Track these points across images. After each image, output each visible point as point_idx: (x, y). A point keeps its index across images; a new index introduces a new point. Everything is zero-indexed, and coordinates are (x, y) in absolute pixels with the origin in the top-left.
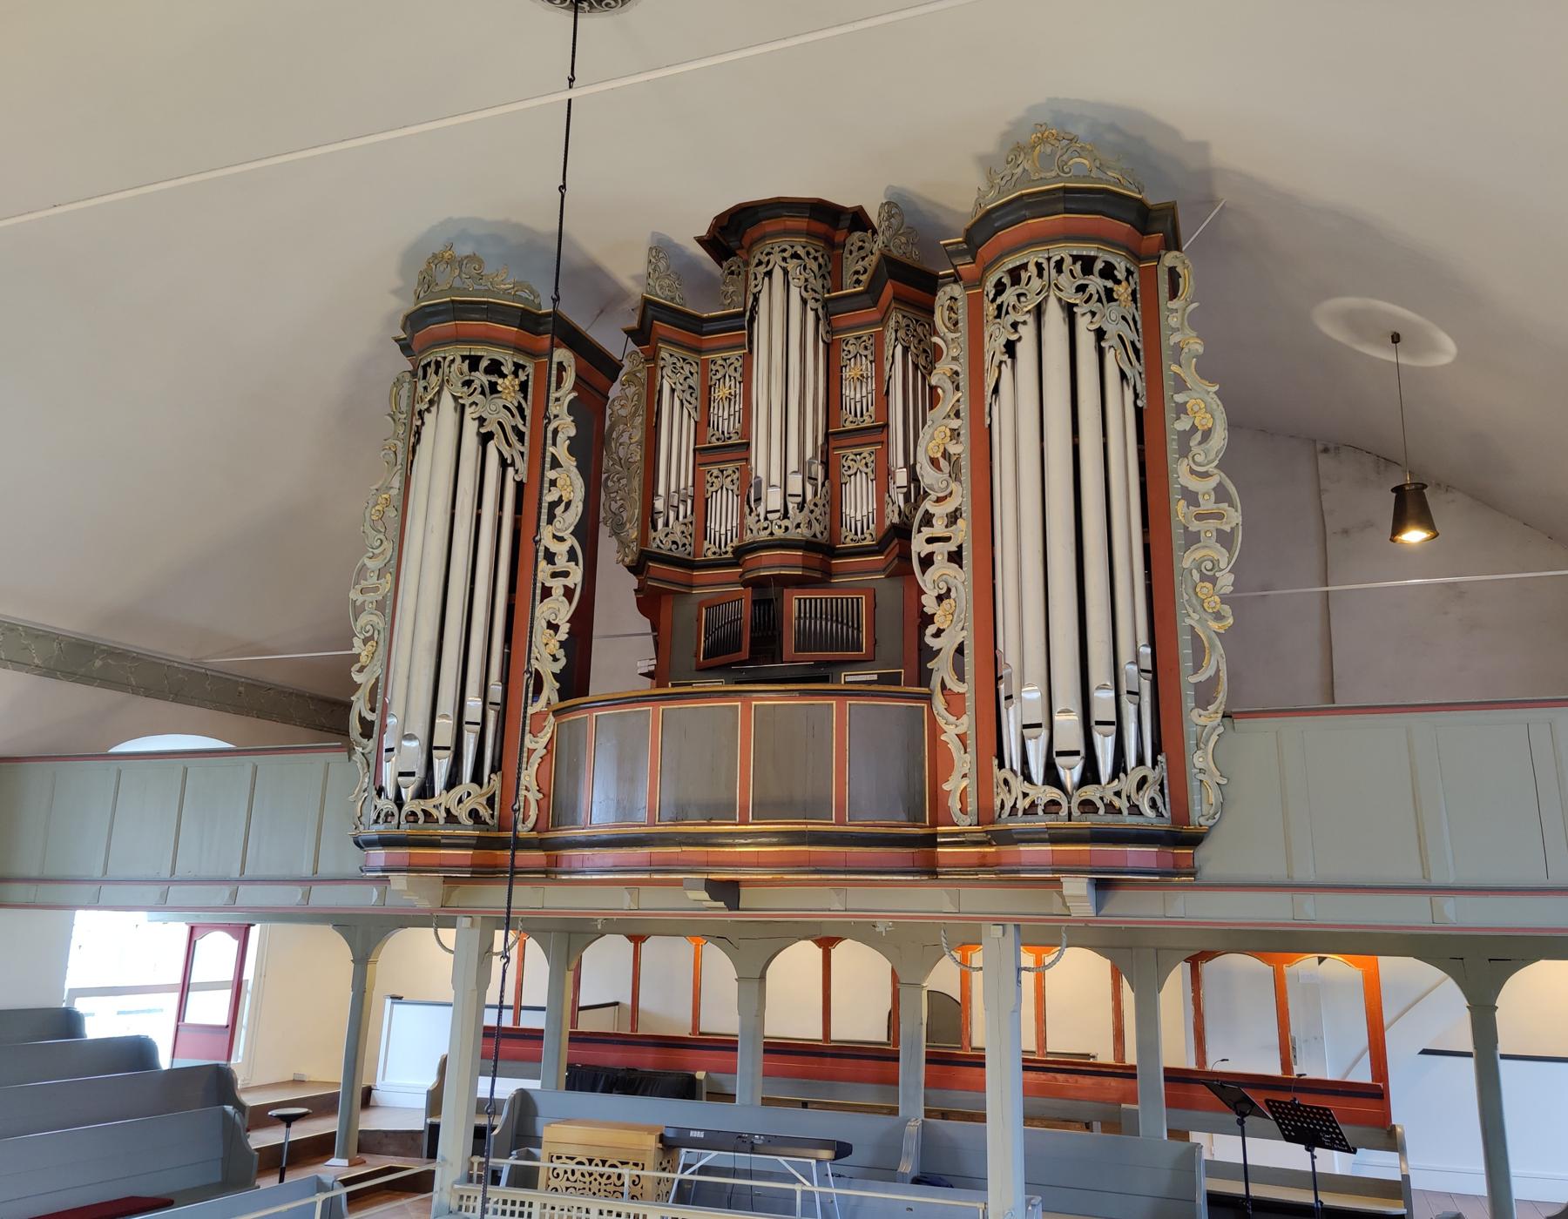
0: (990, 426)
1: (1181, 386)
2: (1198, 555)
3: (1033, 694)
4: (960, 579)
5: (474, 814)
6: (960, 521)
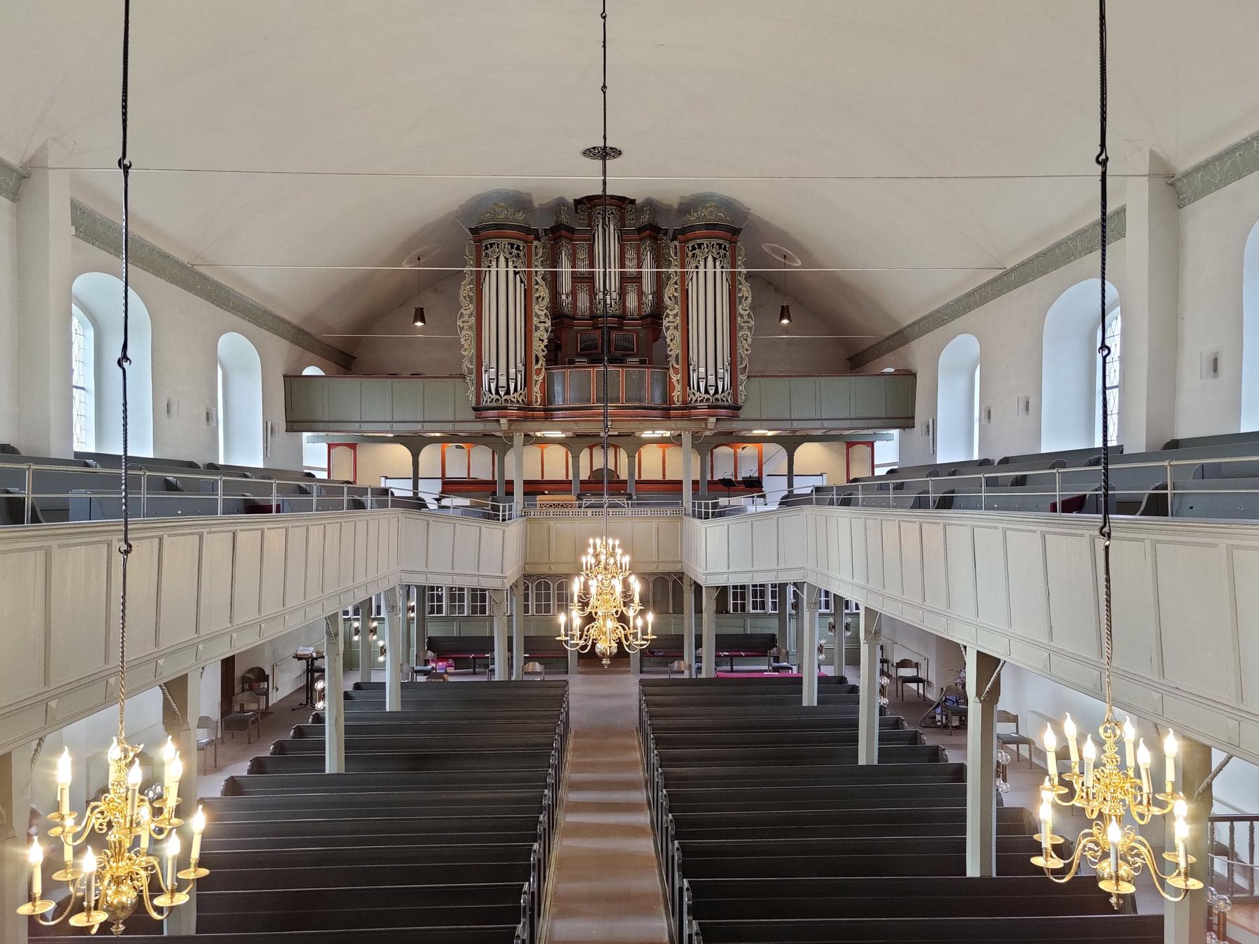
0: (687, 290)
1: (740, 283)
2: (743, 333)
3: (702, 370)
4: (678, 334)
5: (523, 400)
6: (678, 318)
